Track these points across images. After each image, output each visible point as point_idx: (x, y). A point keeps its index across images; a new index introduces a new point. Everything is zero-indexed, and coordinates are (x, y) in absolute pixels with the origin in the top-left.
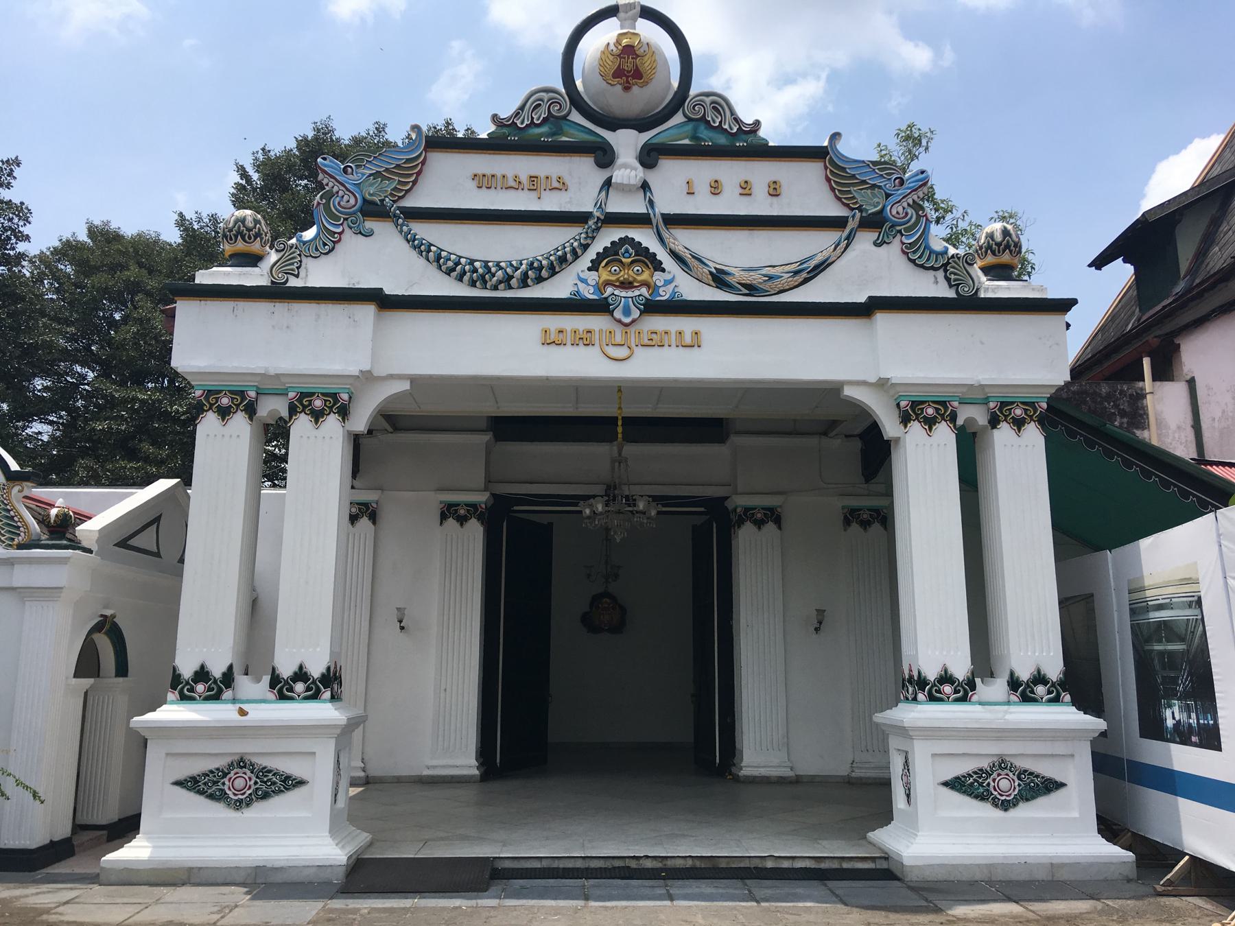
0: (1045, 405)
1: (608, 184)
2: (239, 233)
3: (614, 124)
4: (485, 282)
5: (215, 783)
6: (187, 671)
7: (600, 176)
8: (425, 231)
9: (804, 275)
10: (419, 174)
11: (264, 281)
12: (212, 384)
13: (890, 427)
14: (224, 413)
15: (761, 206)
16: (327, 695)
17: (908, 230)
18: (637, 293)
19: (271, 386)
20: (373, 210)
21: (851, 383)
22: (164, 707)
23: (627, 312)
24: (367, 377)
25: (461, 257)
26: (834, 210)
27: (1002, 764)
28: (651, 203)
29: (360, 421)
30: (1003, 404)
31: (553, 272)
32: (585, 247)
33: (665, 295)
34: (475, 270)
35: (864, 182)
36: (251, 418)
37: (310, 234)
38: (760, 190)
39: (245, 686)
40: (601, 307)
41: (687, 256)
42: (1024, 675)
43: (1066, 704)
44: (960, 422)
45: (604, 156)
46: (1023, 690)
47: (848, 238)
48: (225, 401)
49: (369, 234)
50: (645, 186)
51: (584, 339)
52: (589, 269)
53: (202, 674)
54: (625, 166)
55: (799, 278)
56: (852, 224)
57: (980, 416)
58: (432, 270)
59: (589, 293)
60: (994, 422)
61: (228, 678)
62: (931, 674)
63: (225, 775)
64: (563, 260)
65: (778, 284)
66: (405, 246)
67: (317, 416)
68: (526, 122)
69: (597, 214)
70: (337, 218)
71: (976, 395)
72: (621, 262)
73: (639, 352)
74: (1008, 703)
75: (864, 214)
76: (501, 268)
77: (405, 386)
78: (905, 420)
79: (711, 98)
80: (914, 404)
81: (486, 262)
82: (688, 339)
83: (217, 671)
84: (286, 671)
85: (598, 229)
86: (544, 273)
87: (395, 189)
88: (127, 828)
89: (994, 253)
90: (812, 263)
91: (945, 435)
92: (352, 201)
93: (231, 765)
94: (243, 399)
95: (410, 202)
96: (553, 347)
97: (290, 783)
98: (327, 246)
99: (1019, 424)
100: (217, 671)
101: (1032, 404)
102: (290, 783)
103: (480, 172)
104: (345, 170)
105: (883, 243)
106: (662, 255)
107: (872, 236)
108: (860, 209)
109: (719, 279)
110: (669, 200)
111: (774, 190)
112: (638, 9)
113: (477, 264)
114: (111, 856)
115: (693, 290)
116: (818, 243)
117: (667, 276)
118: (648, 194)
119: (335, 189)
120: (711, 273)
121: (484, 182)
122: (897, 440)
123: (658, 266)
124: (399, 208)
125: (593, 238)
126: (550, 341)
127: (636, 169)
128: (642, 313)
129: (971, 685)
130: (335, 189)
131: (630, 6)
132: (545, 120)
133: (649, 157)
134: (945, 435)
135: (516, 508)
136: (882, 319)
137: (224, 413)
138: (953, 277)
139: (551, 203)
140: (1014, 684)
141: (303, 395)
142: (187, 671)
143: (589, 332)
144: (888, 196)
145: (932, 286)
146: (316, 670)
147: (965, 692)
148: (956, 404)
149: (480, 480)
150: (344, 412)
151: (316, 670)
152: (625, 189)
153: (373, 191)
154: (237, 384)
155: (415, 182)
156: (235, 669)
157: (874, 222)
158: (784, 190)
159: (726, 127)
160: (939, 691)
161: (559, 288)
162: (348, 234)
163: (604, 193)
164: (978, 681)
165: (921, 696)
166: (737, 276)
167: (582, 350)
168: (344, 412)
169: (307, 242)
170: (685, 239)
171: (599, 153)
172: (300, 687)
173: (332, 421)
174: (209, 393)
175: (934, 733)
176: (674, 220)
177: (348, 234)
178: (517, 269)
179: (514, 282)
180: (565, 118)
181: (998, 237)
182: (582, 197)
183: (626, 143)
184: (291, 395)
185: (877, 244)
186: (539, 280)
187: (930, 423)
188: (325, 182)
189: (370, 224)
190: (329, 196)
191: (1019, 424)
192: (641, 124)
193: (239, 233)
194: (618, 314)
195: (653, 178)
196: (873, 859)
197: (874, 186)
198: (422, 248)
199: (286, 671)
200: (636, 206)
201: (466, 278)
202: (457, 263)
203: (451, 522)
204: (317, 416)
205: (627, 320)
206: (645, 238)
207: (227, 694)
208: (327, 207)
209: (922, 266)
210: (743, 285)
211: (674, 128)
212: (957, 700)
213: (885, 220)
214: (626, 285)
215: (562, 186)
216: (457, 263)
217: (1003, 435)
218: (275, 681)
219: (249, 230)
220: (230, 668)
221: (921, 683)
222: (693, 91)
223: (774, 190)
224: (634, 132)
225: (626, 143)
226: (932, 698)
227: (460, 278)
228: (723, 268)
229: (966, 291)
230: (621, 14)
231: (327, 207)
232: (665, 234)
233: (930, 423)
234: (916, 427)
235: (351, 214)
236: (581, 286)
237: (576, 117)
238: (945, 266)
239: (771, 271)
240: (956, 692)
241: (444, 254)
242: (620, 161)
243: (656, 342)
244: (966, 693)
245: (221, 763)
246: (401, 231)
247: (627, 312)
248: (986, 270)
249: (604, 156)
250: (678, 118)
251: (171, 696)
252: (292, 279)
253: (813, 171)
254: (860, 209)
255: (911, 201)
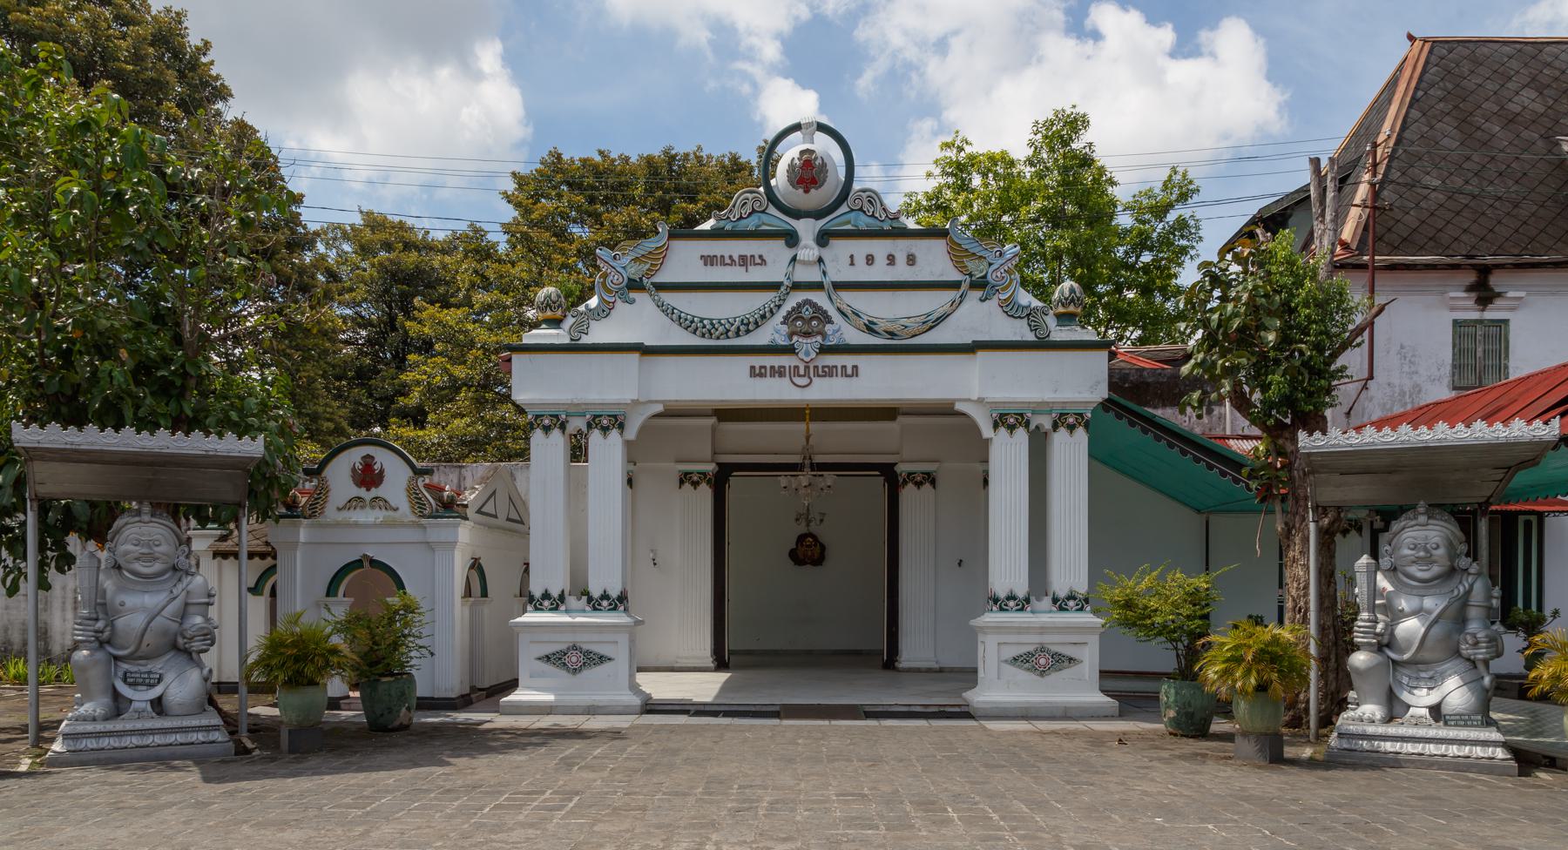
0: (1089, 415)
1: (794, 259)
2: (548, 305)
3: (797, 214)
4: (711, 334)
5: (560, 659)
6: (537, 593)
7: (789, 253)
8: (669, 298)
9: (930, 324)
10: (664, 257)
11: (567, 341)
12: (538, 411)
13: (987, 431)
14: (547, 429)
15: (902, 273)
16: (622, 608)
17: (1003, 289)
18: (814, 340)
19: (577, 410)
20: (635, 285)
21: (960, 400)
22: (526, 615)
23: (807, 354)
24: (636, 403)
25: (694, 317)
26: (954, 276)
27: (1042, 649)
28: (824, 273)
29: (631, 432)
30: (1062, 415)
31: (757, 325)
32: (779, 307)
33: (833, 341)
34: (704, 327)
35: (974, 254)
36: (564, 433)
37: (593, 302)
38: (901, 259)
39: (572, 601)
40: (790, 350)
41: (849, 312)
42: (1062, 594)
43: (1087, 612)
44: (1032, 427)
45: (791, 238)
46: (1060, 604)
47: (961, 297)
48: (547, 422)
49: (632, 302)
50: (820, 260)
51: (779, 372)
52: (782, 323)
53: (546, 596)
54: (806, 247)
55: (926, 327)
56: (964, 287)
57: (1046, 422)
58: (675, 326)
59: (782, 341)
60: (1055, 426)
61: (562, 598)
62: (1002, 595)
63: (565, 654)
64: (763, 317)
65: (910, 331)
66: (658, 311)
67: (605, 430)
68: (737, 217)
69: (786, 283)
70: (609, 291)
71: (1041, 408)
72: (802, 318)
73: (816, 380)
74: (1050, 612)
75: (973, 279)
76: (722, 325)
77: (659, 408)
78: (996, 426)
79: (868, 193)
80: (1002, 415)
81: (711, 320)
82: (849, 371)
83: (555, 593)
84: (596, 594)
85: (788, 294)
86: (751, 327)
87: (648, 270)
88: (512, 685)
89: (1063, 305)
90: (933, 317)
91: (1021, 435)
92: (621, 280)
93: (568, 649)
94: (558, 420)
95: (661, 278)
96: (758, 378)
97: (602, 659)
98: (605, 311)
99: (1071, 428)
100: (555, 593)
101: (1081, 415)
102: (602, 659)
103: (706, 254)
104: (615, 257)
105: (986, 299)
106: (832, 312)
107: (978, 294)
108: (971, 275)
109: (870, 328)
110: (839, 271)
111: (911, 260)
112: (815, 126)
113: (705, 322)
114: (505, 699)
115: (855, 337)
116: (941, 299)
117: (835, 327)
118: (822, 266)
119: (609, 271)
120: (865, 324)
121: (709, 260)
122: (991, 439)
123: (830, 322)
124: (652, 283)
125: (784, 300)
126: (756, 373)
127: (812, 249)
128: (817, 354)
129: (1027, 600)
130: (609, 271)
131: (809, 125)
132: (750, 214)
133: (823, 238)
134: (1021, 435)
135: (735, 474)
136: (981, 354)
137: (547, 429)
138: (1033, 323)
139: (756, 275)
140: (1055, 600)
141: (595, 417)
142: (537, 593)
143: (780, 367)
144: (990, 264)
145: (1019, 331)
146: (614, 593)
147: (1023, 604)
148: (1029, 415)
149: (708, 454)
150: (621, 427)
151: (614, 593)
152: (805, 263)
153: (634, 271)
154: (553, 411)
155: (661, 264)
156: (566, 593)
157: (980, 284)
158: (918, 260)
159: (877, 215)
160: (1006, 605)
161: (761, 338)
162: (619, 304)
163: (790, 268)
164: (1033, 599)
165: (994, 608)
166: (880, 327)
167: (776, 381)
168: (621, 427)
169: (594, 309)
170: (850, 299)
171: (789, 237)
172: (605, 603)
173: (614, 433)
174: (537, 417)
175: (999, 629)
176: (839, 286)
177: (619, 304)
178: (732, 325)
179: (730, 334)
180: (763, 212)
181: (1067, 293)
182: (775, 271)
183: (806, 229)
184: (588, 416)
185: (982, 300)
186: (748, 331)
187: (1011, 428)
188: (601, 265)
189: (632, 295)
190: (605, 276)
191: (1071, 428)
192: (818, 214)
193: (548, 305)
194: (801, 355)
195: (826, 254)
196: (959, 706)
197: (981, 257)
198: (669, 311)
199: (596, 594)
200: (813, 275)
201: (698, 332)
202: (692, 322)
203: (687, 485)
204: (605, 430)
205: (807, 359)
206: (820, 298)
207: (563, 608)
208: (604, 284)
209: (1012, 316)
210: (887, 332)
211: (842, 218)
212: (1017, 610)
213: (988, 283)
214: (807, 334)
215: (763, 262)
216: (692, 322)
217: (1060, 438)
218: (590, 599)
219: (554, 303)
220: (563, 591)
221: (996, 601)
222: (856, 186)
223: (911, 260)
224: (812, 220)
225: (806, 229)
226: (1001, 609)
227: (695, 333)
228: (875, 320)
229: (1041, 334)
230: (803, 130)
231: (604, 284)
232: (834, 297)
233: (1011, 428)
234: (1003, 431)
235: (620, 289)
236: (777, 336)
237: (772, 210)
238: (1028, 315)
239: (903, 322)
240: (1017, 605)
241: (683, 315)
242: (802, 243)
243: (829, 372)
244: (1023, 606)
245: (563, 647)
246: (654, 300)
247: (807, 354)
248: (1059, 316)
249: (791, 238)
250: (844, 209)
251: (529, 608)
252: (584, 336)
253: (939, 245)
254: (971, 275)
255: (1006, 268)
